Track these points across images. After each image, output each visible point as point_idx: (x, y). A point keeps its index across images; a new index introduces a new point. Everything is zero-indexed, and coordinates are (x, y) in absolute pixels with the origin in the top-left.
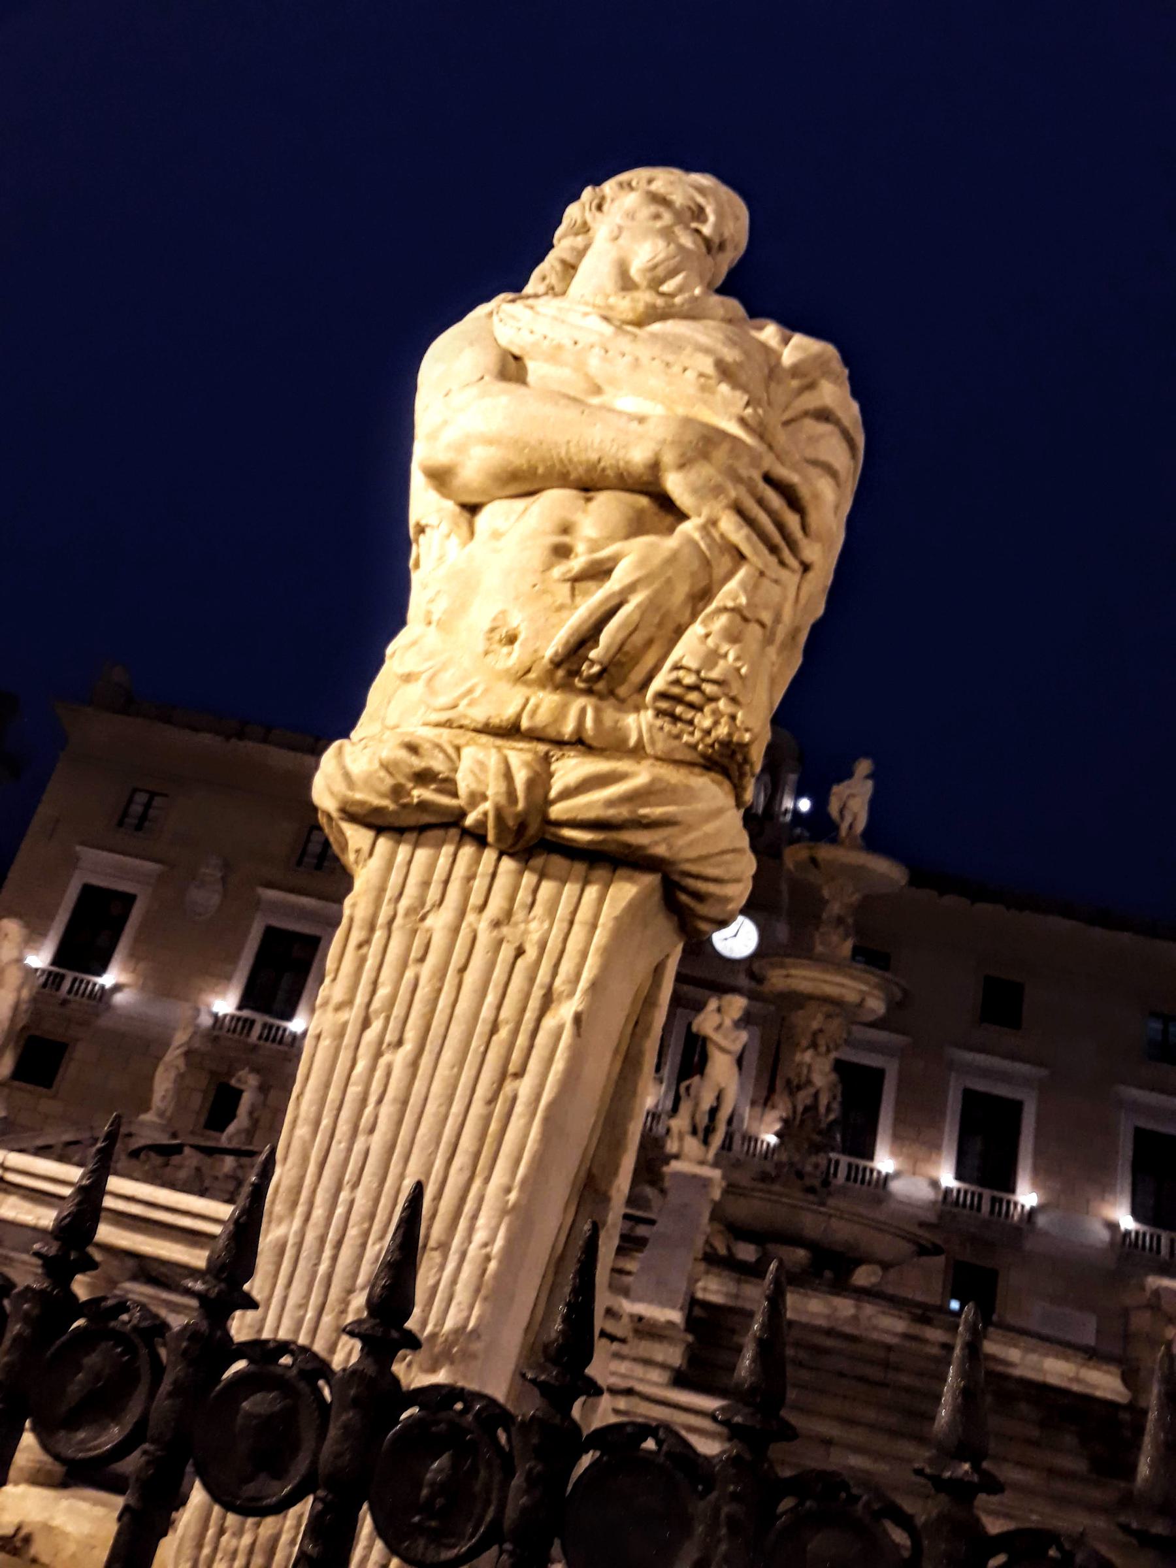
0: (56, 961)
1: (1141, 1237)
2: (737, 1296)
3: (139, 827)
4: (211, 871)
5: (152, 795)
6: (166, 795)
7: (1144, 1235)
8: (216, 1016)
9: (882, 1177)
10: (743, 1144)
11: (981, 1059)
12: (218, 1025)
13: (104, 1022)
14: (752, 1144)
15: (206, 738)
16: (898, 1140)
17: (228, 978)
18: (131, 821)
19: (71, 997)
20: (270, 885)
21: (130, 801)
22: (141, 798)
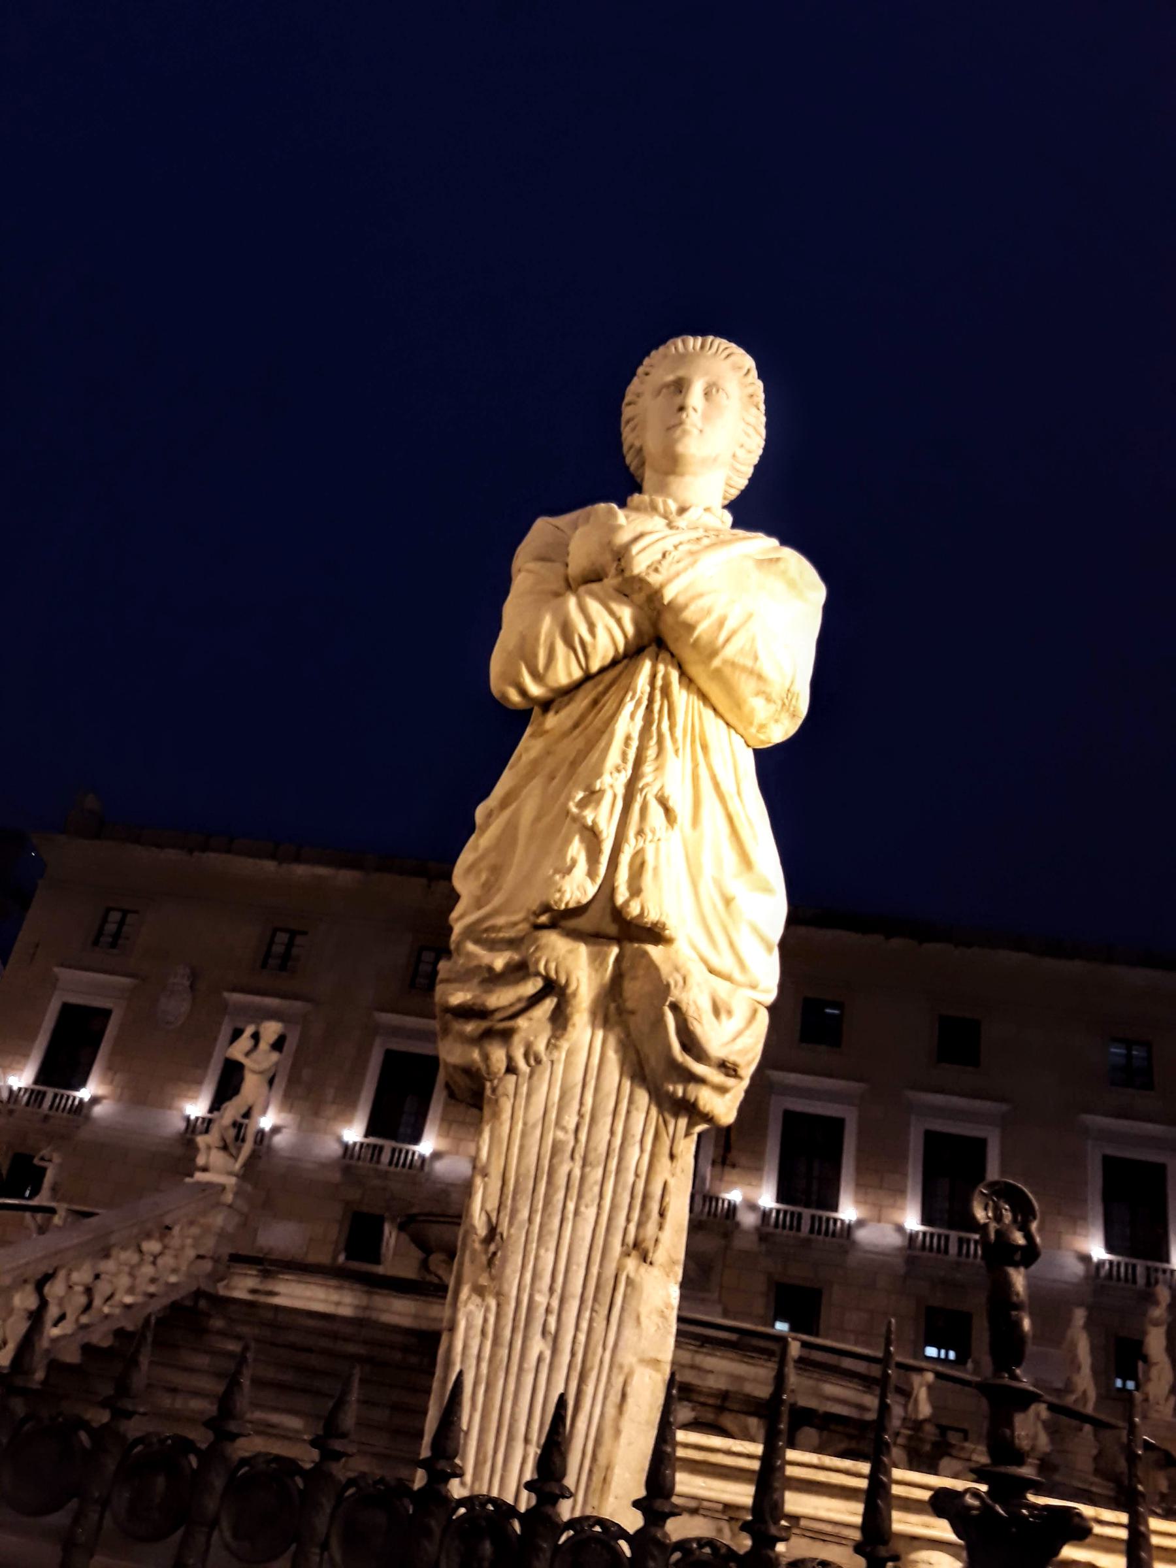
0: (37, 1081)
1: (1115, 1269)
2: (366, 1308)
3: (113, 945)
4: (179, 979)
5: (125, 913)
6: (136, 912)
7: (1119, 1264)
8: (188, 1119)
9: (846, 1226)
10: (704, 1205)
11: (939, 1099)
12: (190, 1129)
13: (84, 1134)
14: (714, 1204)
15: (172, 855)
16: (862, 1188)
17: (199, 1082)
18: (106, 939)
19: (52, 1113)
20: (234, 990)
21: (105, 920)
22: (115, 916)
